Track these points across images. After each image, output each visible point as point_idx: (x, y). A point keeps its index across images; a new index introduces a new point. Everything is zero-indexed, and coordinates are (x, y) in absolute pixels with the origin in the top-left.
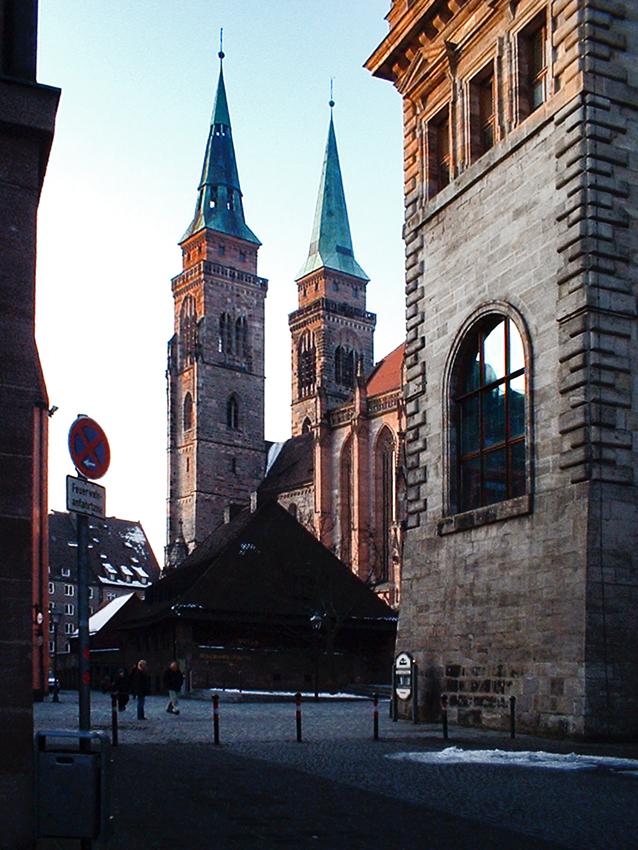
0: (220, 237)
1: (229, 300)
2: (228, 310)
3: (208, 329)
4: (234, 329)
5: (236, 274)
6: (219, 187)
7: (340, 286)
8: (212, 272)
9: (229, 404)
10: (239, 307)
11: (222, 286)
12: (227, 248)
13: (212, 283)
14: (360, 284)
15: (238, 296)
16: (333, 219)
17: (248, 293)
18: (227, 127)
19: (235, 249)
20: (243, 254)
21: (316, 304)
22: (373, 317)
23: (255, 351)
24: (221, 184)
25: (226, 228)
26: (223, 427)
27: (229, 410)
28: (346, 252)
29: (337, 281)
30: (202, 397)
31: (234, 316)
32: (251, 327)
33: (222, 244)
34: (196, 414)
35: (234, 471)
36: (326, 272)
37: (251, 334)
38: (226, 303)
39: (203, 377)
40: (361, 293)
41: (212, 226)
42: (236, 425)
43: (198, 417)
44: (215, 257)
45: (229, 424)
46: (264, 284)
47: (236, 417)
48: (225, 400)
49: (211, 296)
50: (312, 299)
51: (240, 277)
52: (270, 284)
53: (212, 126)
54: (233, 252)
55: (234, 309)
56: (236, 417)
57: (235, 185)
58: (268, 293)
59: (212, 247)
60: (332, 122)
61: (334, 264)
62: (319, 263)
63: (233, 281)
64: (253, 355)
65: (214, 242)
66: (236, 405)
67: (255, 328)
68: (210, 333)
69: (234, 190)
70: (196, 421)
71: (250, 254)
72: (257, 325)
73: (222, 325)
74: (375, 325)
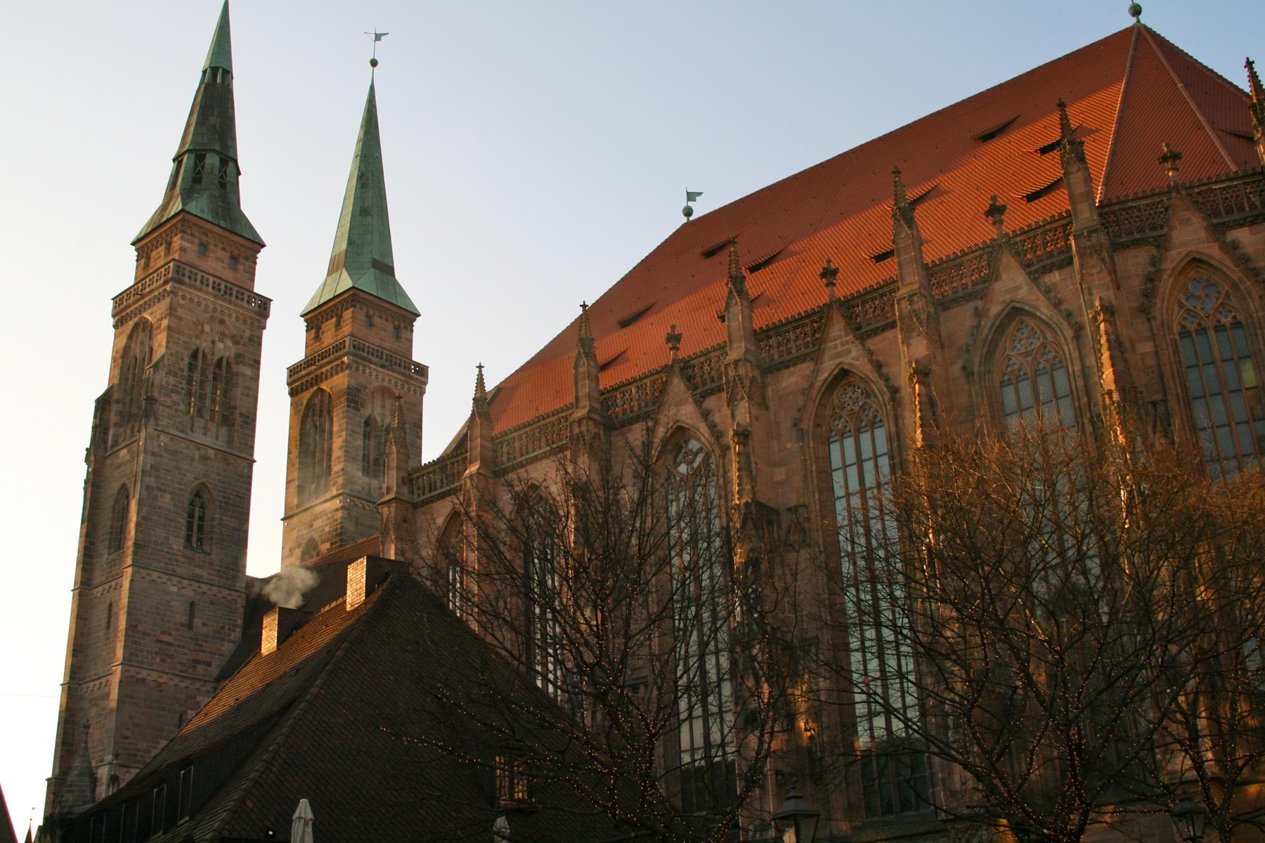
0: (201, 227)
1: (207, 328)
2: (204, 345)
3: (169, 372)
4: (211, 376)
5: (222, 287)
6: (208, 156)
7: (376, 320)
8: (186, 279)
9: (192, 504)
10: (221, 340)
11: (199, 304)
12: (211, 247)
13: (183, 297)
14: (405, 317)
15: (222, 322)
16: (368, 220)
17: (237, 318)
18: (228, 73)
19: (223, 249)
20: (234, 259)
21: (338, 347)
22: (422, 371)
23: (241, 415)
24: (213, 151)
25: (215, 213)
26: (178, 544)
27: (191, 515)
28: (385, 269)
29: (371, 313)
30: (148, 488)
31: (213, 354)
32: (237, 374)
33: (204, 239)
34: (134, 519)
35: (190, 625)
36: (353, 297)
37: (237, 385)
38: (203, 331)
39: (153, 454)
40: (404, 334)
41: (192, 207)
42: (200, 540)
43: (138, 525)
44: (192, 257)
45: (188, 538)
46: (264, 304)
47: (201, 528)
48: (187, 497)
49: (180, 319)
50: (329, 338)
51: (228, 292)
52: (273, 306)
53: (204, 72)
54: (220, 254)
55: (213, 342)
56: (201, 528)
57: (231, 155)
58: (269, 322)
59: (189, 241)
60: (372, 88)
61: (368, 283)
62: (346, 282)
63: (215, 296)
64: (239, 420)
65: (192, 235)
66: (202, 507)
67: (244, 375)
68: (172, 380)
69: (229, 161)
70: (133, 533)
71: (247, 259)
72: (248, 371)
73: (192, 368)
74: (426, 383)
